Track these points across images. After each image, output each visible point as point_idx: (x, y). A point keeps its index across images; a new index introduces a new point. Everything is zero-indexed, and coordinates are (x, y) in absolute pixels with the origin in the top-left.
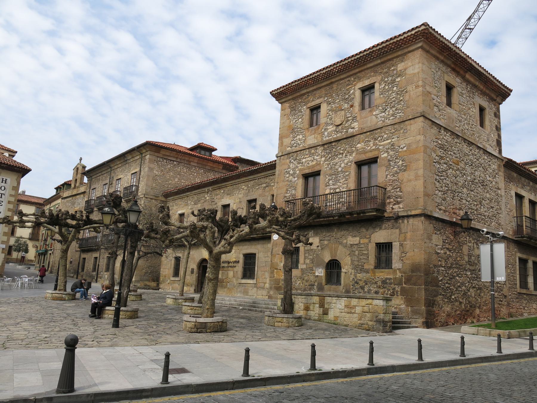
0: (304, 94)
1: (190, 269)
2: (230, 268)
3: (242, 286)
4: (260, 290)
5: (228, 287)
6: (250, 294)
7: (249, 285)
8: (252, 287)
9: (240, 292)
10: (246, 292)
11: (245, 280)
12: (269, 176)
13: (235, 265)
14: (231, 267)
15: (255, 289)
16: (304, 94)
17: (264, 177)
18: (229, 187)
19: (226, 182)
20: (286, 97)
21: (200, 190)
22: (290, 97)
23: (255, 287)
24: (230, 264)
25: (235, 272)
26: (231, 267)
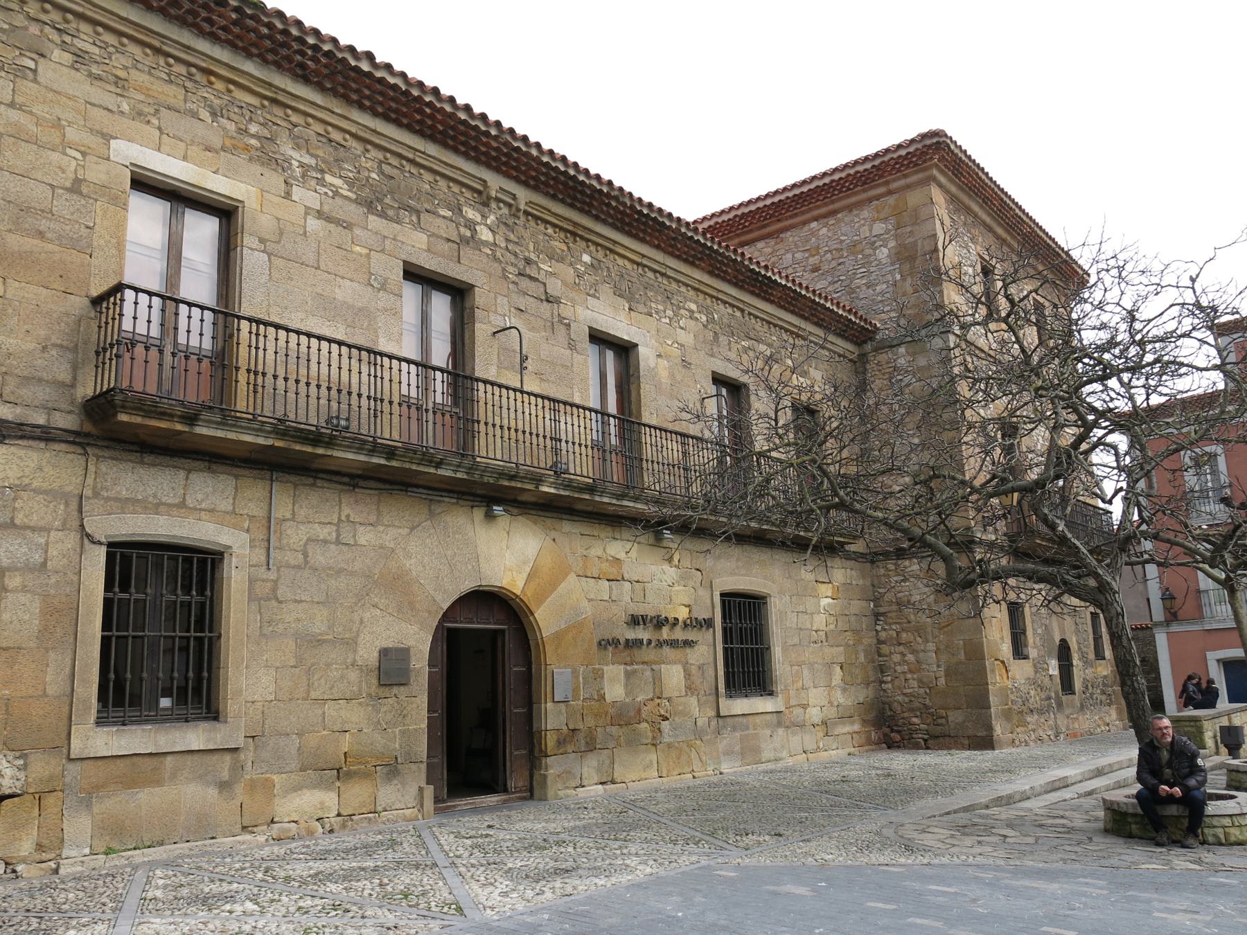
0: (968, 210)
1: (373, 658)
2: (667, 650)
3: (734, 729)
4: (794, 734)
5: (667, 739)
6: (767, 754)
7: (758, 719)
8: (768, 725)
9: (729, 753)
10: (749, 752)
11: (745, 701)
12: (781, 328)
13: (691, 635)
14: (673, 644)
15: (781, 731)
16: (968, 210)
17: (769, 323)
18: (620, 261)
19: (629, 234)
20: (951, 180)
21: (432, 149)
22: (953, 189)
23: (779, 724)
24: (665, 633)
25: (694, 670)
26: (673, 644)
